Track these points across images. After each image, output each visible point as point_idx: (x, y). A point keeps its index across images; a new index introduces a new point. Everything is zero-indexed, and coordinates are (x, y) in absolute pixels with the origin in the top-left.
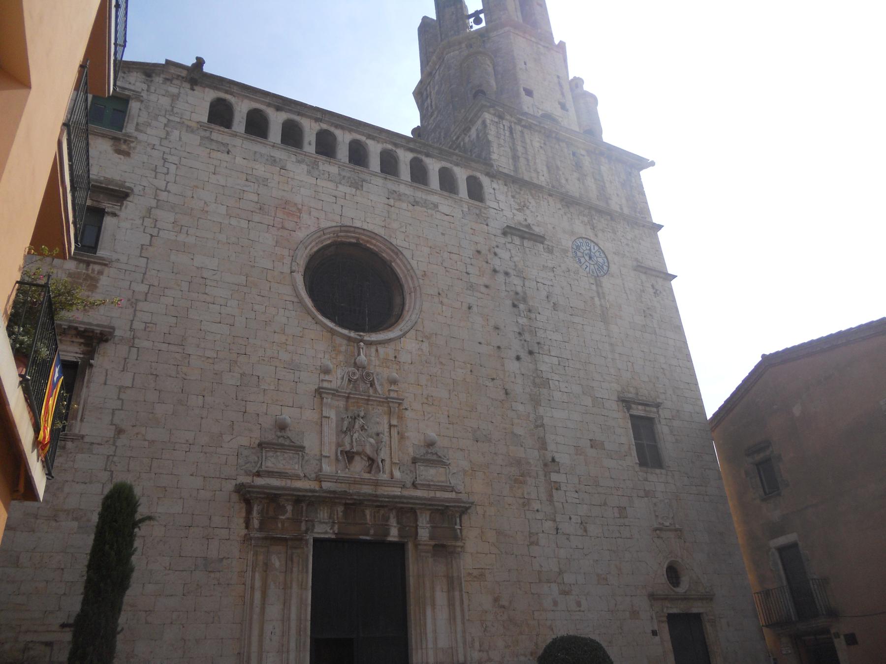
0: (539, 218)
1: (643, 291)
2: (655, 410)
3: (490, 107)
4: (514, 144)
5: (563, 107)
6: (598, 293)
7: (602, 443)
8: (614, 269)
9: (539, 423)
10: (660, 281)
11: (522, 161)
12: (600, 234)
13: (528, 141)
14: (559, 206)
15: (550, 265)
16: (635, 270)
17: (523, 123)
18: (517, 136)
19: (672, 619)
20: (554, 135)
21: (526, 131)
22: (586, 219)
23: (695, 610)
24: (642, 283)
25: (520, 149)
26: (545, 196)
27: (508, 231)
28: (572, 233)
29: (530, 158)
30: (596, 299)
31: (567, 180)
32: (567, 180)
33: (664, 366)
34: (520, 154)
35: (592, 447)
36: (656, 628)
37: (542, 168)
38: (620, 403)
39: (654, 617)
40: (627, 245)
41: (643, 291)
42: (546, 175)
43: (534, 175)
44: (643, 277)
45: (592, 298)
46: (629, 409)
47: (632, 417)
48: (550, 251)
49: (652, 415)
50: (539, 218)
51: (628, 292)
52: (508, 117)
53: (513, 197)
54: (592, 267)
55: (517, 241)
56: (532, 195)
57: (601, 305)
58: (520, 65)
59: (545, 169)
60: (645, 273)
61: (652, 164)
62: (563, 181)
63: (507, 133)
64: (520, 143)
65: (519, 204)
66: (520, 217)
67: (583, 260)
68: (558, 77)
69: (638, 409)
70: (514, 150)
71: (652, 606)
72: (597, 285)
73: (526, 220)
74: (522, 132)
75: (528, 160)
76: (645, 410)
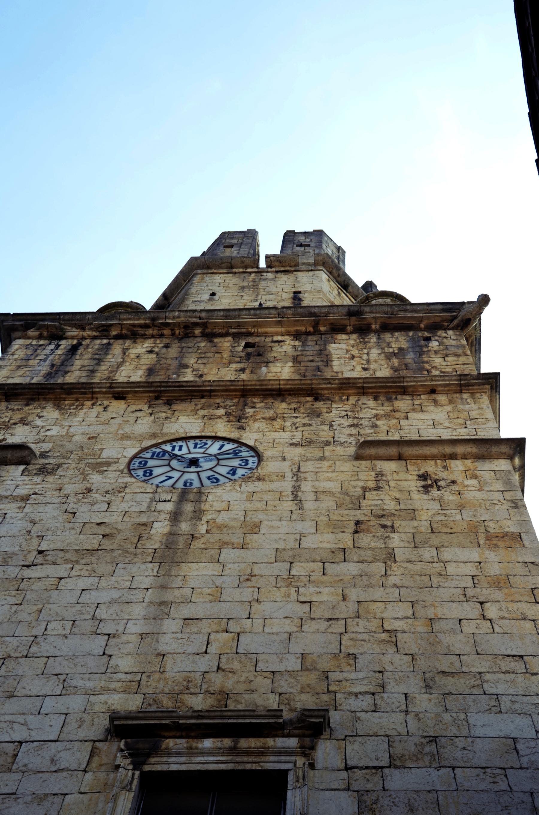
1: (378, 488)
2: (292, 742)
10: (457, 466)
15: (22, 491)
16: (358, 457)
17: (114, 333)
20: (197, 332)
22: (221, 412)
26: (106, 403)
33: (398, 625)
38: (113, 750)
46: (138, 759)
47: (144, 776)
48: (43, 471)
49: (271, 764)
56: (58, 407)
57: (171, 534)
60: (400, 457)
61: (484, 300)
69: (191, 752)
76: (233, 750)
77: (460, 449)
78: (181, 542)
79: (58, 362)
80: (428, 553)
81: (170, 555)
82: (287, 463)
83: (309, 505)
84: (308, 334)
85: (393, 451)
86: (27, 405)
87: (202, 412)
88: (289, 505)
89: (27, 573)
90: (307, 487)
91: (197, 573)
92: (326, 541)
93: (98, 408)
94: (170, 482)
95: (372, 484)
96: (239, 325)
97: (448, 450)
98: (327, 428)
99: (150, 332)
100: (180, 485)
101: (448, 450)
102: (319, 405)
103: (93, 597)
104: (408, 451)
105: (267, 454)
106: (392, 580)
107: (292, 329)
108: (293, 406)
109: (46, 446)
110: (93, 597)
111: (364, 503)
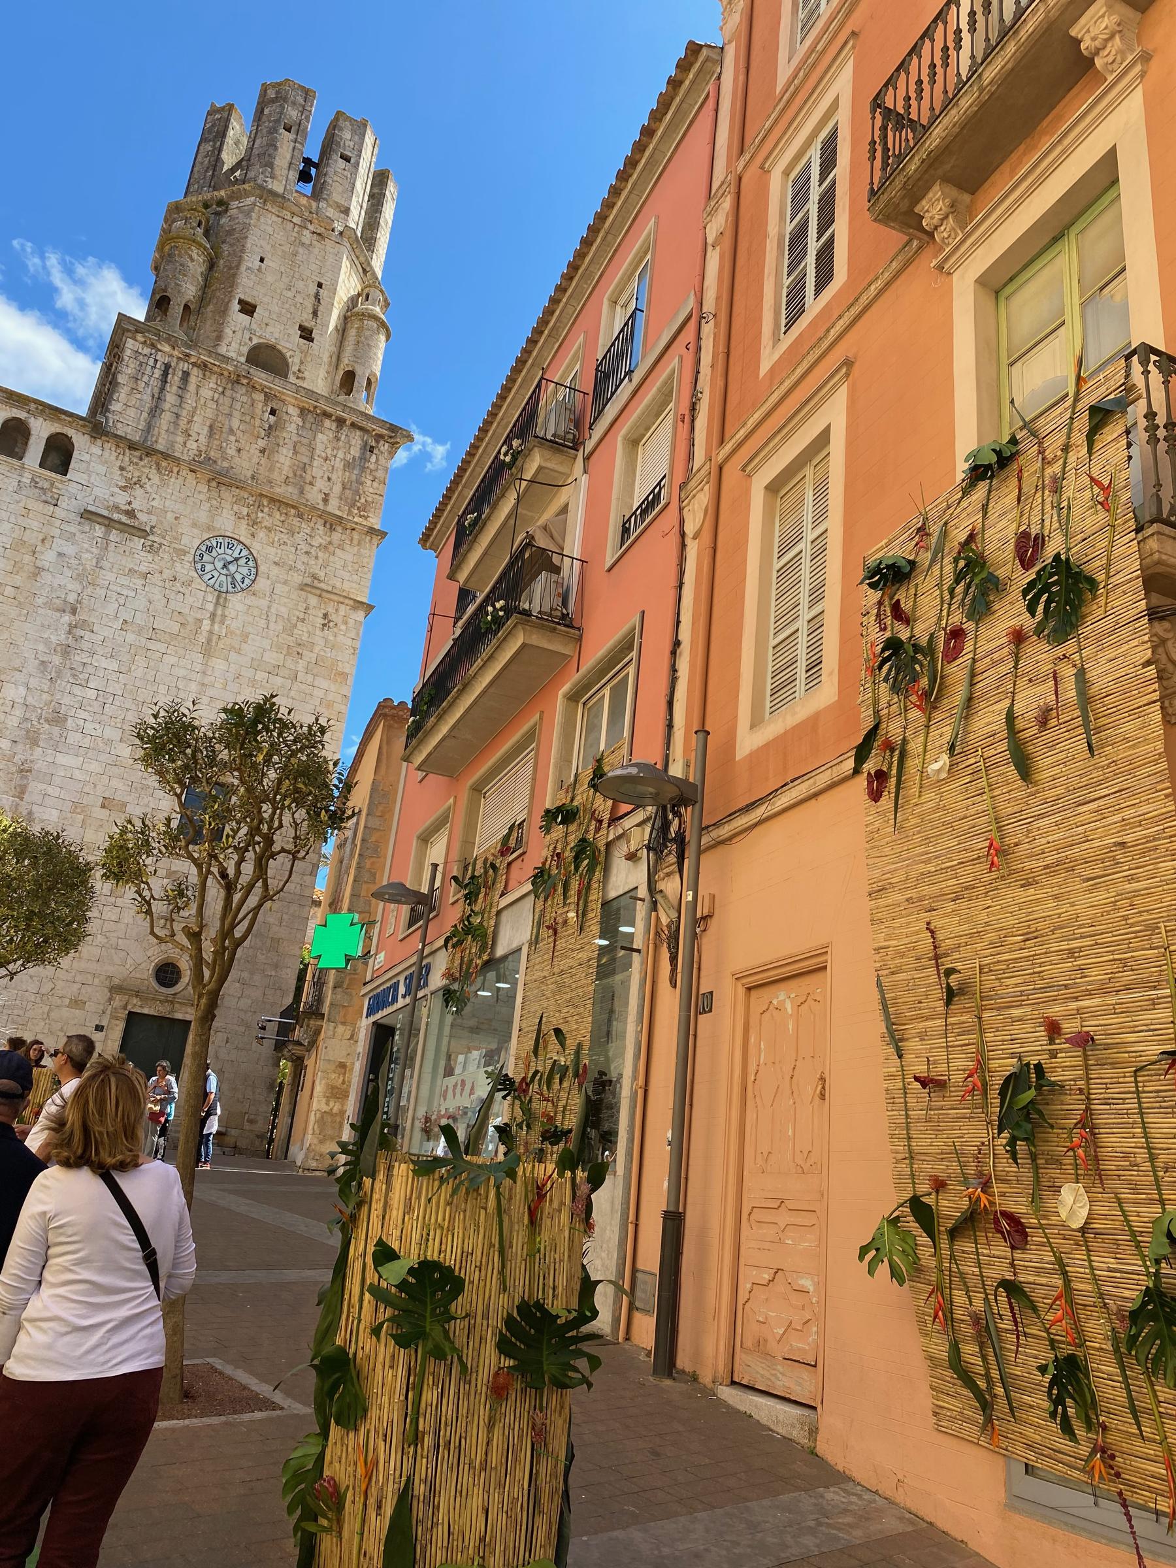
0: (154, 503)
1: (303, 620)
3: (137, 331)
4: (162, 389)
5: (307, 334)
6: (213, 616)
7: (125, 804)
8: (262, 584)
9: (26, 766)
11: (165, 419)
12: (262, 534)
13: (192, 387)
14: (203, 488)
15: (143, 568)
18: (175, 379)
19: (133, 1019)
21: (195, 371)
22: (245, 511)
23: (179, 1016)
24: (307, 608)
25: (170, 398)
26: (184, 473)
27: (87, 515)
28: (209, 528)
29: (184, 413)
30: (207, 622)
31: (239, 451)
32: (239, 451)
34: (166, 406)
35: (103, 806)
36: (104, 1023)
37: (200, 428)
39: (108, 1012)
40: (307, 553)
41: (303, 620)
42: (203, 439)
43: (180, 439)
44: (313, 601)
45: (200, 621)
48: (153, 549)
50: (154, 503)
51: (273, 618)
52: (167, 348)
53: (122, 469)
54: (223, 578)
55: (99, 531)
57: (211, 632)
58: (251, 261)
59: (206, 430)
62: (231, 452)
63: (158, 373)
64: (175, 389)
65: (127, 480)
66: (121, 499)
67: (209, 567)
68: (320, 285)
70: (159, 399)
71: (110, 1000)
72: (217, 603)
73: (130, 503)
74: (186, 375)
75: (178, 416)
77: (347, 601)
78: (215, 638)
79: (156, 390)
80: (310, 678)
81: (208, 650)
82: (269, 582)
83: (272, 626)
84: (309, 411)
85: (318, 592)
86: (141, 459)
87: (236, 507)
88: (263, 623)
89: (152, 645)
90: (273, 610)
91: (218, 664)
92: (272, 658)
93: (180, 480)
94: (213, 581)
95: (301, 615)
96: (270, 388)
97: (341, 599)
98: (293, 550)
99: (215, 369)
100: (217, 586)
101: (341, 599)
102: (296, 521)
103: (176, 671)
104: (324, 594)
105: (262, 568)
106: (292, 693)
107: (302, 404)
108: (282, 518)
109: (154, 520)
110: (176, 671)
111: (296, 631)
